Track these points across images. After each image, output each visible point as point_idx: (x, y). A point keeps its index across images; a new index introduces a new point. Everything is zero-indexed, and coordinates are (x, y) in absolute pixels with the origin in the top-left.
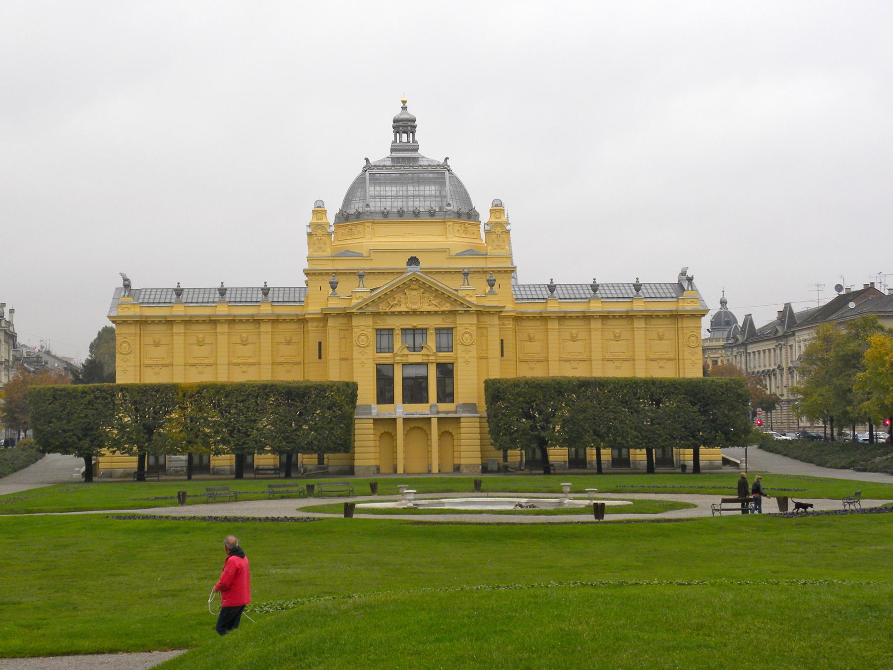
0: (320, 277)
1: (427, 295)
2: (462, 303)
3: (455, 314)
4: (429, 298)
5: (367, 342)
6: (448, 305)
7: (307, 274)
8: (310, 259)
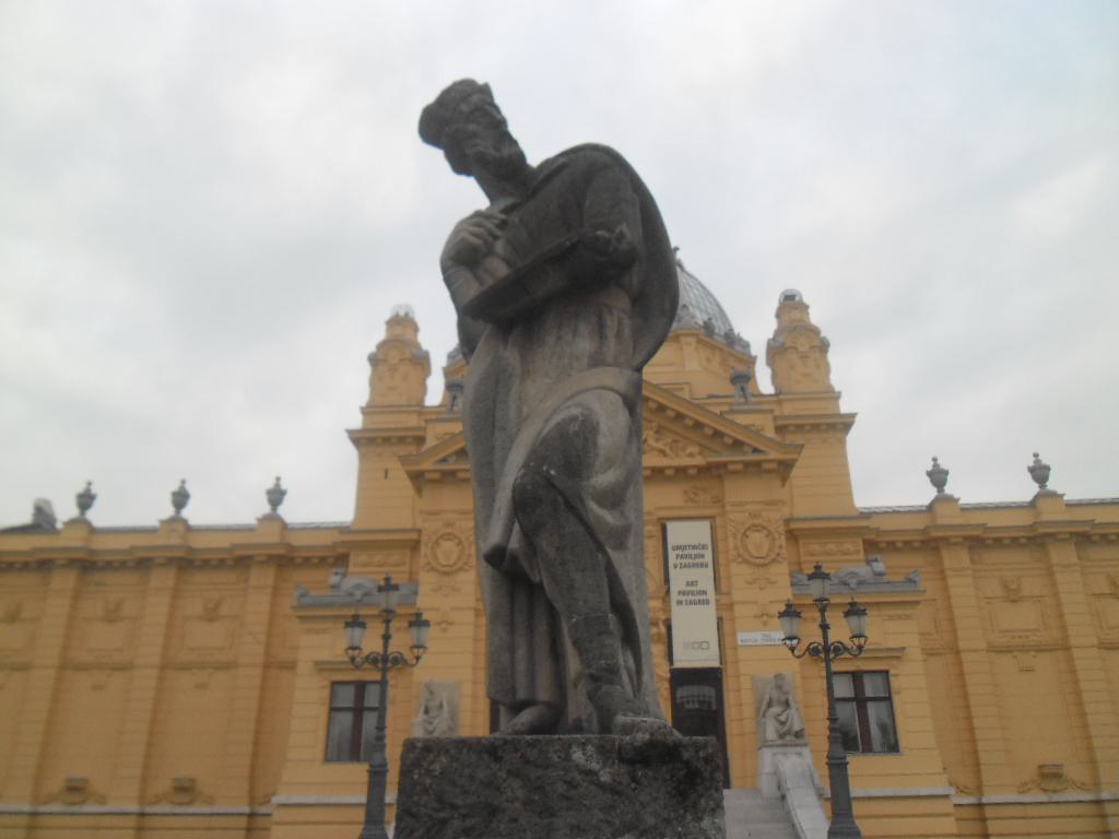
2: (738, 444)
3: (719, 477)
5: (459, 559)
6: (694, 449)
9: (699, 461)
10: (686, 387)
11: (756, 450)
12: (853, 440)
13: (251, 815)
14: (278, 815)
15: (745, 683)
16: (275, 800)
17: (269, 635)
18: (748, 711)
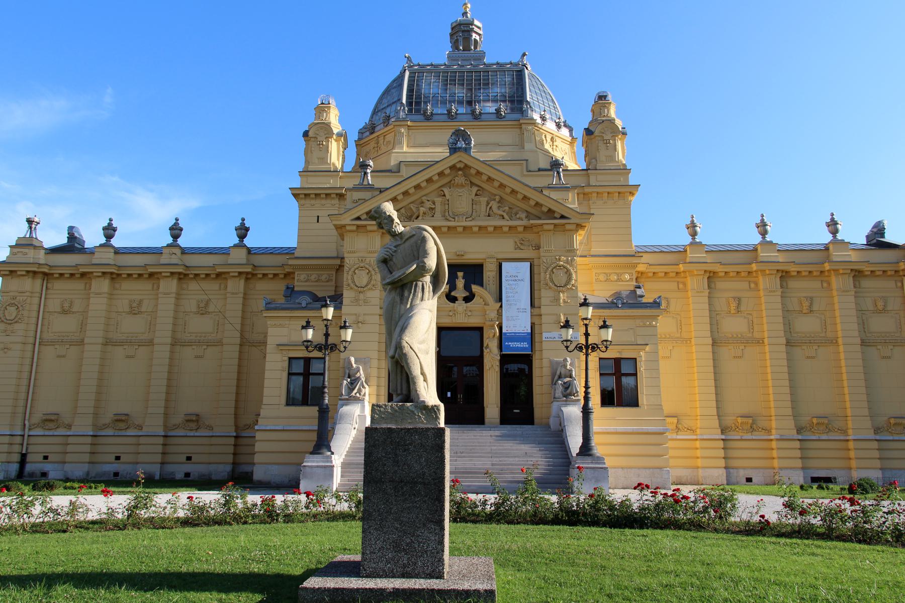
0: (318, 202)
1: (484, 200)
4: (488, 203)
7: (295, 195)
8: (305, 173)
9: (525, 222)
10: (524, 162)
11: (563, 217)
12: (635, 201)
13: (236, 437)
14: (259, 436)
15: (545, 363)
16: (256, 427)
17: (242, 325)
18: (547, 380)
